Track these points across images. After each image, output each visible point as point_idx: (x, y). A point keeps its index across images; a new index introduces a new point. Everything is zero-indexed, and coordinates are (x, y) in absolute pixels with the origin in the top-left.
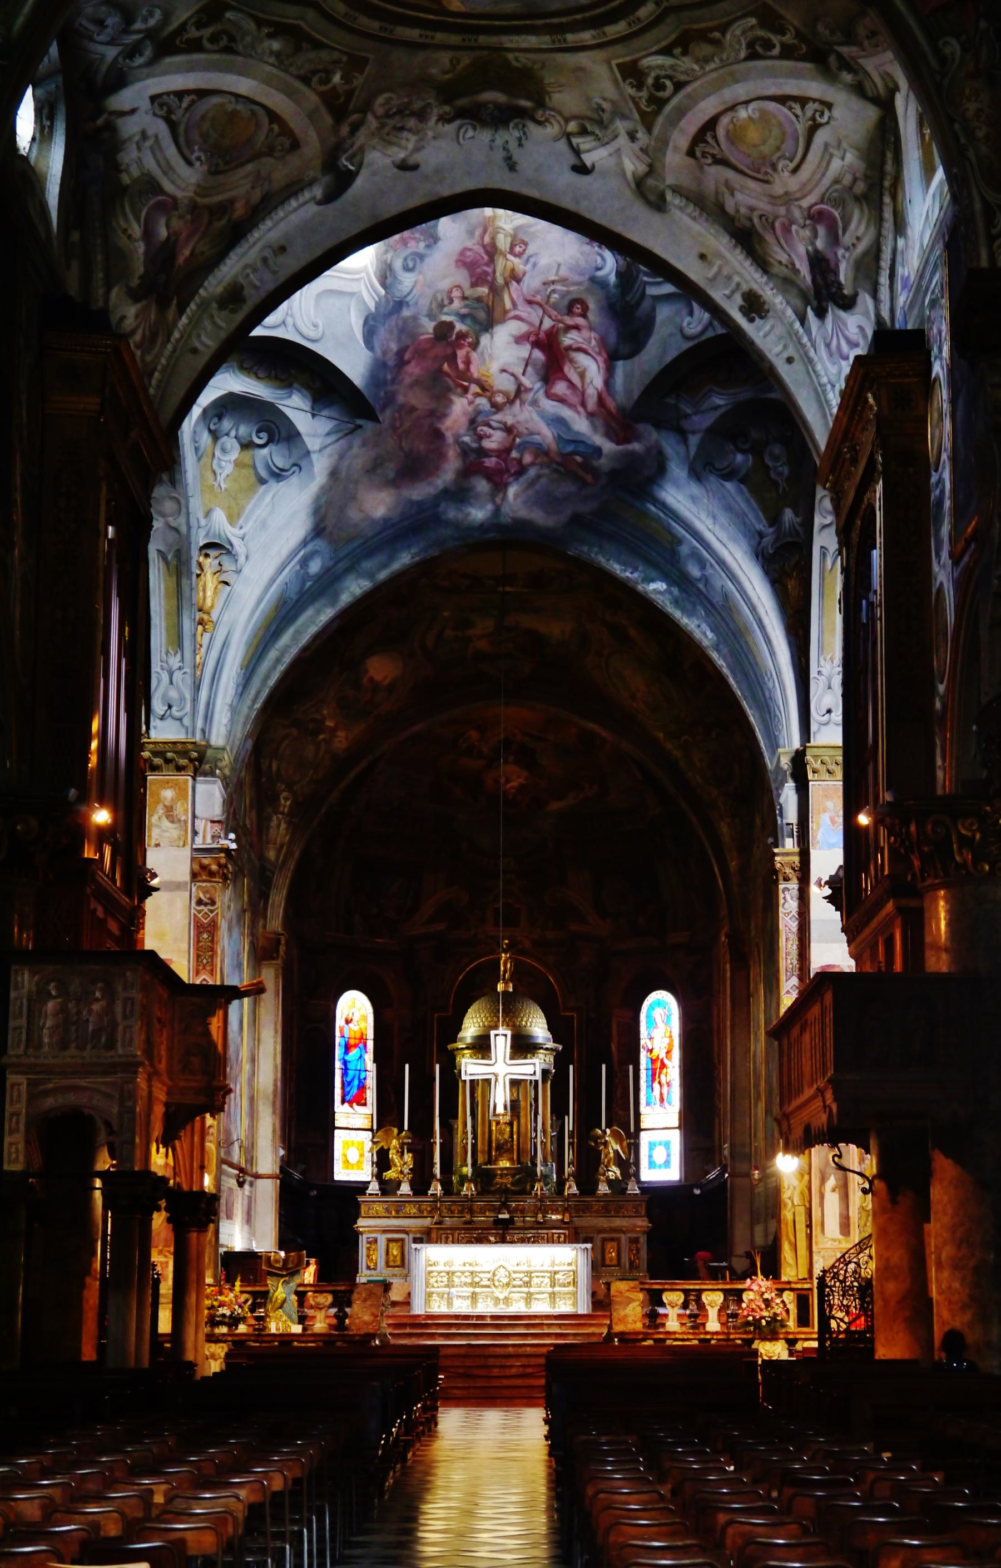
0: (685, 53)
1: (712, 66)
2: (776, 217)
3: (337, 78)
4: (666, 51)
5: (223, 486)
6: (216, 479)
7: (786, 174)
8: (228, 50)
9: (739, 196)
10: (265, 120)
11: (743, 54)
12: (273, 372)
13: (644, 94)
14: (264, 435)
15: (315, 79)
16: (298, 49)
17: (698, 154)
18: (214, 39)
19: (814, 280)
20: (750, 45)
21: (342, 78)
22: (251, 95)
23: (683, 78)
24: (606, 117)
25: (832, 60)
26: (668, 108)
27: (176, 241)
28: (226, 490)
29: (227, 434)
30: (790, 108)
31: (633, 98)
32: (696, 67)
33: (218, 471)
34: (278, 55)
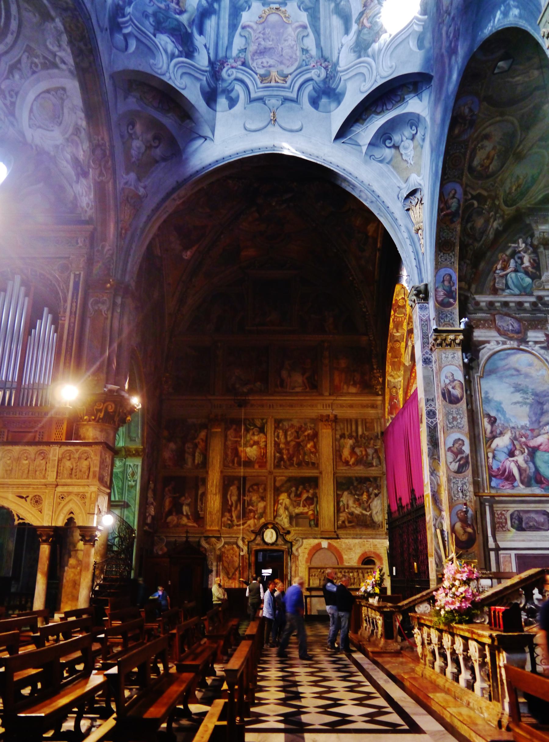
3: (36, 60)
5: (412, 163)
6: (408, 163)
8: (17, 94)
10: (47, 95)
12: (393, 102)
14: (414, 128)
15: (35, 69)
16: (20, 69)
18: (11, 97)
21: (36, 58)
22: (36, 95)
27: (74, 155)
28: (414, 163)
29: (402, 141)
33: (407, 159)
34: (21, 78)
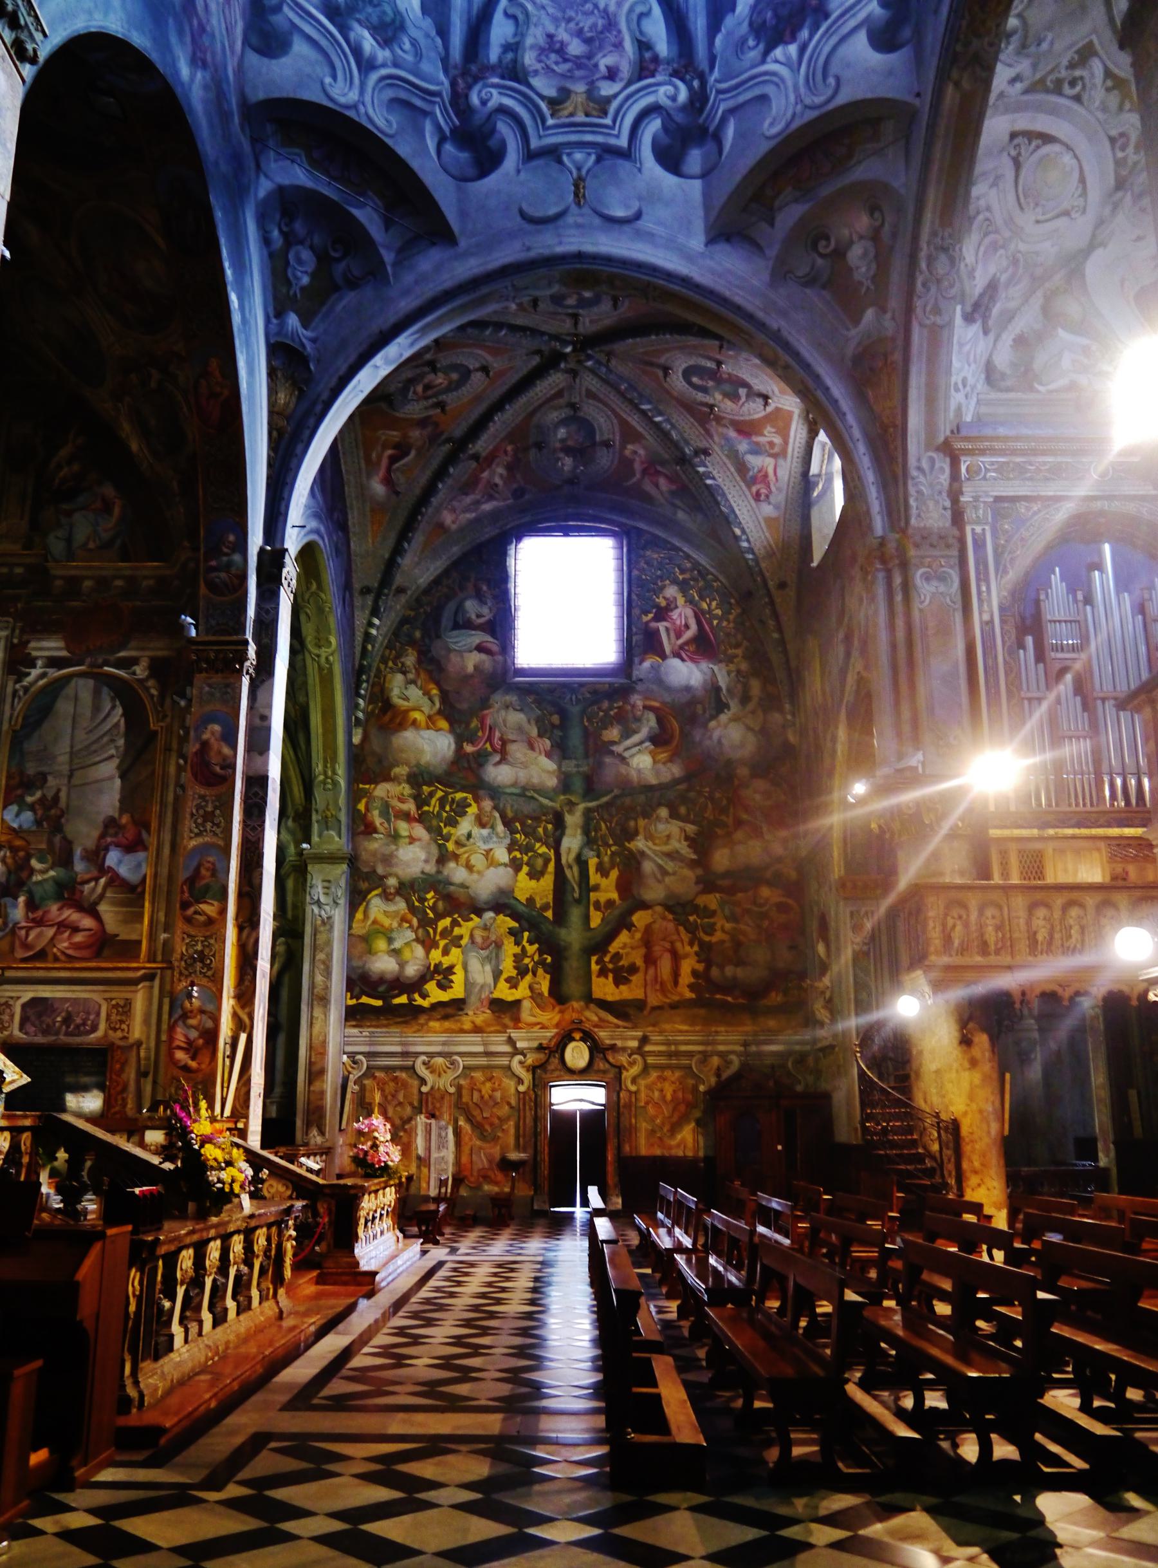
0: (1108, 90)
1: (1100, 115)
2: (997, 231)
4: (1108, 74)
7: (1034, 218)
9: (993, 192)
11: (1114, 133)
13: (1063, 73)
17: (1016, 141)
19: (982, 295)
20: (1122, 135)
23: (1085, 97)
24: (1033, 49)
25: (1120, 194)
26: (1053, 98)
30: (1077, 188)
31: (1058, 66)
32: (1097, 104)
